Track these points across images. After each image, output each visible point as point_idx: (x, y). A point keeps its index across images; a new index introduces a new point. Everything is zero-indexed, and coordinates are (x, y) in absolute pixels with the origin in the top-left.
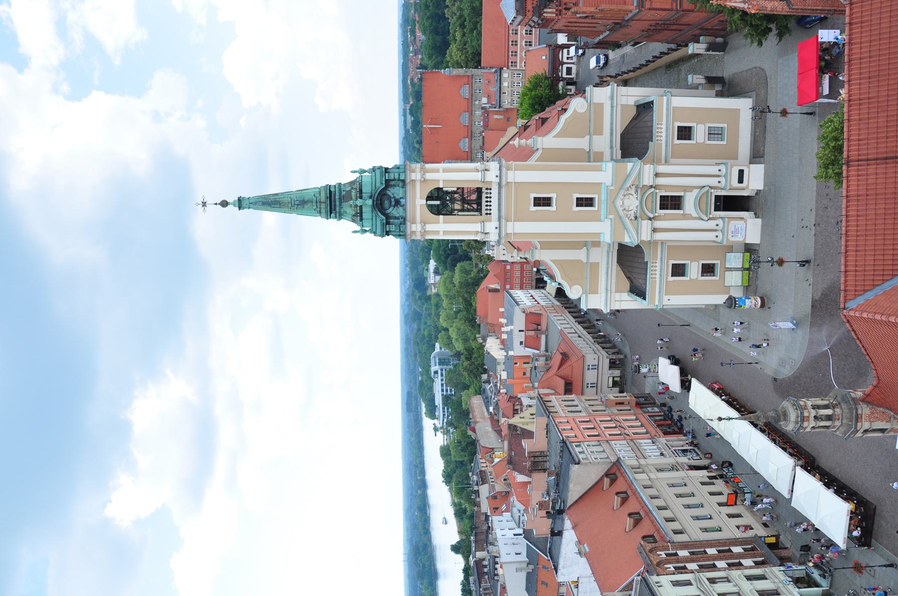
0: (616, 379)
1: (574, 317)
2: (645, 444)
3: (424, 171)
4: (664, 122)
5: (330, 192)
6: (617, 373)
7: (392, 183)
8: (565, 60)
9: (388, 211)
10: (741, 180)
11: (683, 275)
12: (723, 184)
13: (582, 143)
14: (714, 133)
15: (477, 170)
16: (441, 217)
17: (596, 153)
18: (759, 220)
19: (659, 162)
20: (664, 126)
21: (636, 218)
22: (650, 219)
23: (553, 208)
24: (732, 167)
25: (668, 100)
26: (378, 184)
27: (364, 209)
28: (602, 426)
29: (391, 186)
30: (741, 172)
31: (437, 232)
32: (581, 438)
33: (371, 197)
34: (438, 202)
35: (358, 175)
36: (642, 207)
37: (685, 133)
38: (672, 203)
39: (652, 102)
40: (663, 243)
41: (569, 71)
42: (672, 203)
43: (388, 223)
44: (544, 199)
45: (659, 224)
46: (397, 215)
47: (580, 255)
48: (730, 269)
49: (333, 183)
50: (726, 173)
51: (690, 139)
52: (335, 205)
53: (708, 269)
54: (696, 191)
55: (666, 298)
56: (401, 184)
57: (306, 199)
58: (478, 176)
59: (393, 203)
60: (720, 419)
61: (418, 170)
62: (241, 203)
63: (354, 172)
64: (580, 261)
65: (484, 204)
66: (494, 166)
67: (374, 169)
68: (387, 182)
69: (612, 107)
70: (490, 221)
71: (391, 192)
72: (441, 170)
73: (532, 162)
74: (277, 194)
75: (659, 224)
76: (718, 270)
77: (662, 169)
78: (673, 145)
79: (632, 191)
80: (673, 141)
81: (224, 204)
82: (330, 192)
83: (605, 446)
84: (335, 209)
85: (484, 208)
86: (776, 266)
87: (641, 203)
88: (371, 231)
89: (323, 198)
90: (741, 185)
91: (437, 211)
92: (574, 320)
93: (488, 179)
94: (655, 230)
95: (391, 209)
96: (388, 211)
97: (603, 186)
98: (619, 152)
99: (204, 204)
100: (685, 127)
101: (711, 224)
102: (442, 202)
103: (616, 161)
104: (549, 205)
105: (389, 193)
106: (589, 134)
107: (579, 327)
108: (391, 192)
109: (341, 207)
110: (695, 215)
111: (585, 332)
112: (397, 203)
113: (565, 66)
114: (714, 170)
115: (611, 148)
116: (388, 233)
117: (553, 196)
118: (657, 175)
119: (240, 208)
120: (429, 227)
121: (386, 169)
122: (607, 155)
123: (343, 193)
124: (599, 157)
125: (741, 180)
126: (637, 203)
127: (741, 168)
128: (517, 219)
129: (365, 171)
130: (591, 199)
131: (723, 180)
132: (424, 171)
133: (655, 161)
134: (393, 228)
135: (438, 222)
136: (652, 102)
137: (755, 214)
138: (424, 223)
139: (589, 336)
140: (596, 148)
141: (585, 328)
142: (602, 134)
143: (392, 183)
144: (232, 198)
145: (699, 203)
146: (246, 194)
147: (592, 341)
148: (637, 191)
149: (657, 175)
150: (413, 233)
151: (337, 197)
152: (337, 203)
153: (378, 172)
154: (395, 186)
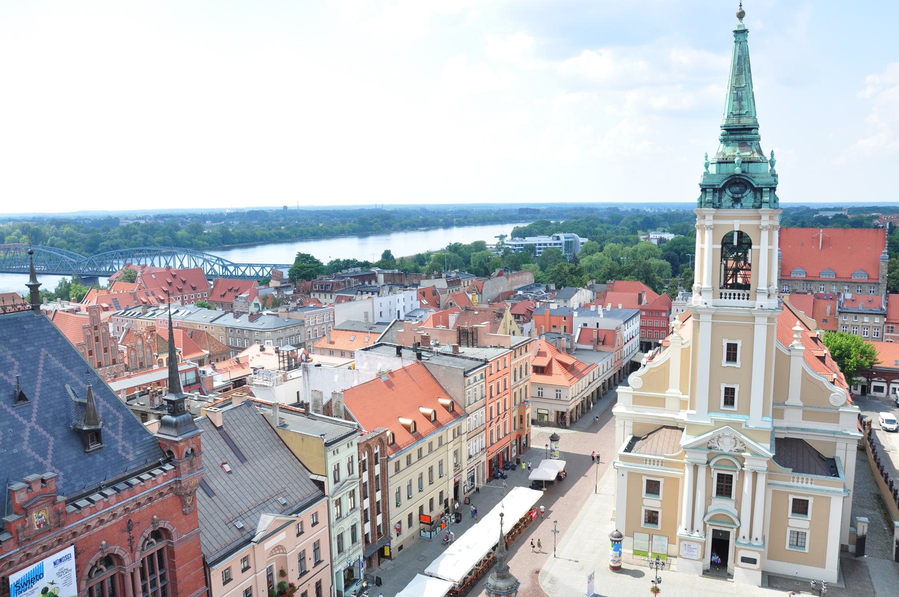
0: (546, 417)
1: (609, 379)
2: (480, 441)
3: (771, 229)
5: (751, 129)
6: (552, 419)
7: (758, 195)
8: (892, 386)
9: (727, 191)
10: (744, 560)
12: (740, 540)
13: (794, 397)
14: (798, 538)
15: (769, 286)
16: (720, 246)
17: (782, 411)
19: (769, 477)
20: (809, 485)
21: (710, 448)
22: (708, 463)
23: (724, 363)
24: (760, 552)
25: (839, 492)
26: (757, 180)
27: (730, 165)
28: (500, 400)
29: (755, 194)
30: (754, 561)
31: (703, 242)
32: (489, 379)
33: (743, 172)
34: (735, 243)
35: (769, 158)
36: (721, 455)
37: (800, 507)
38: (724, 486)
39: (837, 475)
40: (683, 477)
41: (879, 389)
42: (724, 486)
43: (715, 190)
44: (735, 355)
45: (702, 472)
46: (723, 200)
48: (651, 539)
49: (760, 131)
50: (753, 546)
51: (793, 512)
52: (736, 134)
53: (652, 518)
54: (735, 512)
56: (757, 204)
57: (744, 103)
58: (762, 286)
59: (736, 196)
60: (502, 515)
61: (772, 223)
62: (741, 33)
63: (772, 154)
65: (733, 291)
66: (774, 302)
67: (774, 175)
68: (760, 190)
69: (834, 433)
70: (714, 298)
71: (749, 194)
72: (771, 247)
73: (776, 343)
74: (750, 71)
75: (702, 472)
76: (651, 527)
77: (762, 480)
78: (788, 493)
79: (739, 446)
80: (791, 493)
81: (741, 15)
82: (751, 129)
83: (481, 402)
84: (731, 134)
85: (728, 291)
86: (652, 585)
88: (706, 174)
89: (745, 121)
90: (739, 559)
91: (726, 242)
92: (606, 378)
93: (758, 296)
95: (730, 193)
96: (727, 191)
97: (746, 417)
98: (783, 437)
100: (807, 508)
101: (699, 524)
102: (736, 248)
103: (773, 433)
104: (728, 359)
105: (747, 192)
106: (805, 406)
107: (599, 384)
108: (749, 194)
109: (733, 141)
110: (710, 509)
111: (594, 389)
112: (736, 201)
113: (885, 385)
114: (757, 532)
115: (788, 428)
116: (704, 190)
117: (738, 364)
118: (755, 474)
119: (736, 32)
120: (708, 234)
121: (774, 189)
122: (779, 423)
123: (749, 143)
124: (778, 413)
125: (744, 560)
126: (726, 451)
127: (758, 562)
129: (772, 166)
130: (732, 404)
132: (771, 229)
133: (770, 474)
134: (709, 198)
135: (714, 243)
136: (837, 475)
137: (707, 571)
138: (714, 228)
139: (589, 393)
140: (788, 413)
141: (598, 389)
142: (803, 419)
143: (758, 195)
144: (747, 23)
146: (750, 38)
147: (585, 396)
148: (739, 451)
149: (755, 474)
150: (704, 217)
151: (745, 136)
152: (738, 137)
153: (771, 180)
154: (755, 198)
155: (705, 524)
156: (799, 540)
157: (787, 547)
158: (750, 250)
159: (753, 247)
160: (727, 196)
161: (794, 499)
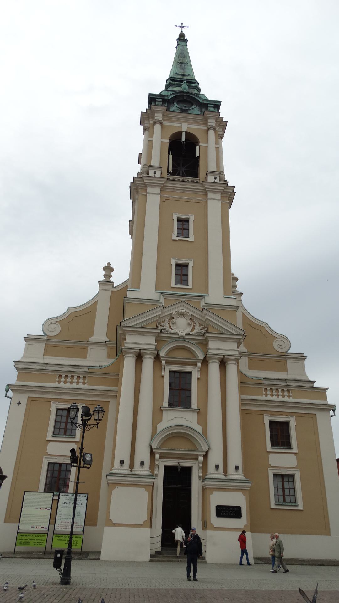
4: (291, 400)
12: (211, 472)
18: (148, 558)
20: (286, 399)
38: (180, 393)
42: (180, 393)
47: (100, 333)
54: (199, 429)
64: (92, 335)
87: (181, 338)
90: (213, 511)
94: (139, 358)
96: (176, 104)
101: (143, 454)
105: (193, 107)
112: (184, 111)
114: (236, 457)
118: (223, 363)
126: (182, 333)
128: (162, 201)
131: (220, 475)
137: (158, 553)
145: (179, 435)
149: (223, 363)
154: (201, 111)
155: (152, 454)
157: (273, 506)
158: (197, 147)
159: (200, 144)
161: (271, 423)
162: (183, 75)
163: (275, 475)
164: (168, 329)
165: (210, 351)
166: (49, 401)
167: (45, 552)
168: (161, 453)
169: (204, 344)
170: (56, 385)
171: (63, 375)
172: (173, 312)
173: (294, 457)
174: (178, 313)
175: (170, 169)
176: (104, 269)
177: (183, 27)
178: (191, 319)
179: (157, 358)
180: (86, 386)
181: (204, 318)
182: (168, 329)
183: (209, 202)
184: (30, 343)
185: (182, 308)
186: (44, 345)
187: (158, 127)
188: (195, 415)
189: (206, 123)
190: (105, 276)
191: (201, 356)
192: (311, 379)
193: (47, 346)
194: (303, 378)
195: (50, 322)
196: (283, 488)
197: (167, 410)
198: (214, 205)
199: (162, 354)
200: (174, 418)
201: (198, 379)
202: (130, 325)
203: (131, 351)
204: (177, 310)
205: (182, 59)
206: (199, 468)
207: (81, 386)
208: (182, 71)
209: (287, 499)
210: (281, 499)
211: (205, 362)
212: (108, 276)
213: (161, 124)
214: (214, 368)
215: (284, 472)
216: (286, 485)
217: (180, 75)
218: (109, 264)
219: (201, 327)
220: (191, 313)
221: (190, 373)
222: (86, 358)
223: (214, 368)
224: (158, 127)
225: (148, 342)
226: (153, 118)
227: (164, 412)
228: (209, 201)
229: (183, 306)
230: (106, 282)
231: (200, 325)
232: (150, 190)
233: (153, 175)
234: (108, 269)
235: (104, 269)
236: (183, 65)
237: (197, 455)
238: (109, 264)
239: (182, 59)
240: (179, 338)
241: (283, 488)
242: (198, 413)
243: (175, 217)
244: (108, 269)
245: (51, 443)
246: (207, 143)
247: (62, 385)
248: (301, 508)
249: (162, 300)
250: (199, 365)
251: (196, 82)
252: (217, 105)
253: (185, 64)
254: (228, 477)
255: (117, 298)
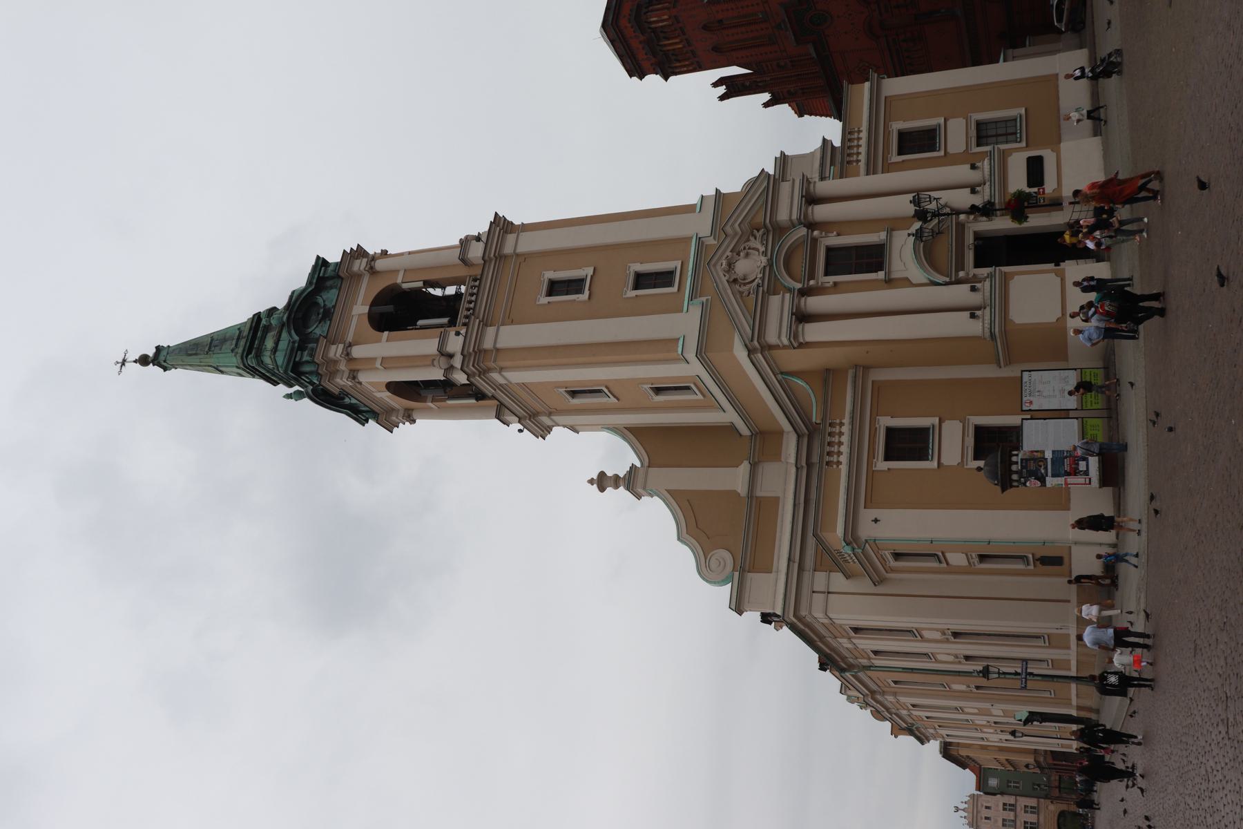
4: (864, 127)
7: (329, 283)
11: (922, 455)
20: (864, 135)
45: (815, 303)
47: (735, 479)
55: (866, 515)
62: (160, 358)
64: (734, 493)
75: (815, 303)
81: (144, 360)
94: (803, 317)
99: (123, 363)
101: (960, 294)
105: (320, 300)
112: (328, 314)
135: (379, 341)
154: (331, 288)
156: (1000, 132)
158: (405, 286)
159: (399, 281)
160: (317, 330)
161: (900, 153)
162: (238, 339)
163: (978, 145)
164: (755, 283)
165: (794, 217)
166: (872, 473)
167: (1110, 418)
168: (957, 271)
169: (779, 230)
170: (844, 468)
171: (827, 458)
172: (724, 279)
173: (951, 123)
174: (728, 272)
175: (445, 320)
176: (602, 489)
177: (123, 363)
178: (738, 254)
179: (804, 293)
180: (846, 421)
181: (736, 234)
182: (755, 283)
183: (520, 250)
184: (746, 600)
185: (718, 267)
186: (750, 575)
187: (357, 352)
188: (895, 233)
189: (358, 277)
190: (617, 487)
191: (803, 231)
192: (819, 144)
193: (753, 569)
194: (818, 156)
195: (706, 571)
196: (997, 136)
197: (890, 272)
198: (527, 244)
199: (799, 286)
200: (903, 256)
201: (839, 235)
202: (749, 331)
203: (794, 327)
204: (721, 274)
205: (198, 353)
206: (975, 220)
207: (845, 429)
208: (228, 343)
209: (1010, 131)
210: (1010, 138)
211: (811, 226)
212: (616, 481)
213: (350, 345)
214: (821, 212)
215: (973, 133)
216: (990, 133)
217: (236, 345)
218: (591, 482)
219: (752, 238)
220: (728, 253)
221: (829, 250)
222: (777, 499)
223: (821, 212)
224: (357, 352)
225: (778, 308)
226: (336, 362)
227: (895, 275)
228: (519, 250)
229: (715, 265)
230: (631, 482)
231: (748, 240)
232: (488, 344)
233: (461, 338)
234: (602, 482)
235: (602, 489)
236: (215, 343)
237: (958, 224)
238: (591, 482)
239: (198, 353)
240: (771, 266)
241: (997, 136)
242: (893, 230)
243: (545, 300)
244: (602, 482)
245: (943, 461)
246: (398, 271)
247: (844, 459)
248: (1023, 111)
249: (704, 299)
250: (816, 233)
251: (257, 317)
252: (321, 263)
253: (212, 340)
254: (987, 177)
255: (664, 452)
